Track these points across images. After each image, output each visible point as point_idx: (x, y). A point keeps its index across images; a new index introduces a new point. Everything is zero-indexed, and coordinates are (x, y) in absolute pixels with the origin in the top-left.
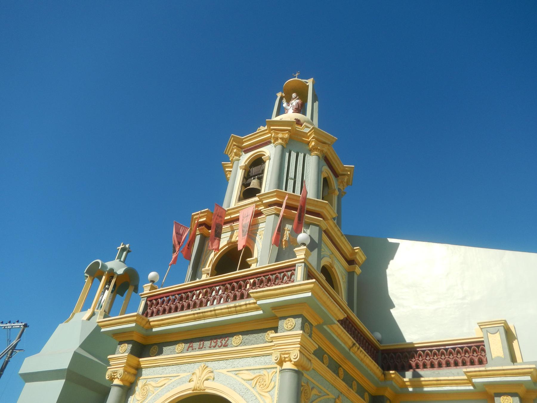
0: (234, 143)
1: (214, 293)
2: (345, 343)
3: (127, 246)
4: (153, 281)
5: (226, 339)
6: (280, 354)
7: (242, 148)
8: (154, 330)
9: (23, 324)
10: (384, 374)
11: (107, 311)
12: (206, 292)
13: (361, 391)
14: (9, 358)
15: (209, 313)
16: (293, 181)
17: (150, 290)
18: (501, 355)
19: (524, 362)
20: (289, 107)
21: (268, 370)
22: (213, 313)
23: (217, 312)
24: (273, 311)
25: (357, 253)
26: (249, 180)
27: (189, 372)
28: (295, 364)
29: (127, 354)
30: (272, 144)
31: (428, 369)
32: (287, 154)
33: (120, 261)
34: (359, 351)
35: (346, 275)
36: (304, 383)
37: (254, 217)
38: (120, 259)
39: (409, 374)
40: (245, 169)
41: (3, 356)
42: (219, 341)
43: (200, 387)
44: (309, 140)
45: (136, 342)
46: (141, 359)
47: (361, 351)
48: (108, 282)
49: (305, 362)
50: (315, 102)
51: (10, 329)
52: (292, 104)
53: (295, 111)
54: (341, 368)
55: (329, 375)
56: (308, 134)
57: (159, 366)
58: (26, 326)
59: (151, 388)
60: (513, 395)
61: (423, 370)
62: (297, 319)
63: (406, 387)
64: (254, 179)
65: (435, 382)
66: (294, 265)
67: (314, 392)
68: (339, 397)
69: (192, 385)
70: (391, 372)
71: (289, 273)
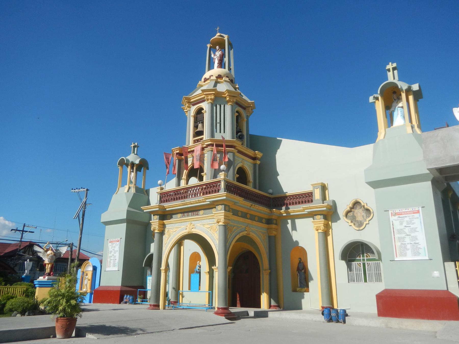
0: (186, 101)
1: (189, 192)
2: (248, 206)
3: (136, 144)
4: (160, 185)
5: (197, 212)
7: (191, 103)
8: (167, 209)
9: (86, 189)
10: (270, 210)
11: (135, 184)
12: (186, 191)
13: (260, 220)
14: (85, 209)
15: (188, 203)
16: (219, 124)
17: (161, 190)
19: (330, 199)
20: (215, 57)
21: (215, 224)
22: (190, 203)
23: (191, 202)
24: (213, 203)
25: (257, 154)
26: (197, 124)
27: (185, 225)
28: (223, 223)
29: (158, 220)
30: (206, 102)
32: (215, 107)
33: (135, 154)
34: (255, 207)
35: (251, 165)
36: (230, 226)
37: (202, 151)
38: (134, 153)
39: (284, 208)
40: (194, 117)
41: (81, 208)
42: (195, 212)
44: (226, 96)
45: (161, 215)
46: (164, 221)
47: (256, 206)
48: (132, 168)
49: (227, 221)
50: (231, 50)
51: (78, 192)
52: (217, 55)
53: (219, 61)
54: (248, 214)
55: (242, 220)
56: (225, 93)
57: (172, 223)
58: (87, 190)
60: (320, 215)
62: (222, 206)
63: (282, 214)
64: (200, 123)
65: (293, 211)
66: (220, 181)
67: (235, 228)
68: (247, 226)
69: (187, 231)
70: (274, 210)
71: (219, 184)
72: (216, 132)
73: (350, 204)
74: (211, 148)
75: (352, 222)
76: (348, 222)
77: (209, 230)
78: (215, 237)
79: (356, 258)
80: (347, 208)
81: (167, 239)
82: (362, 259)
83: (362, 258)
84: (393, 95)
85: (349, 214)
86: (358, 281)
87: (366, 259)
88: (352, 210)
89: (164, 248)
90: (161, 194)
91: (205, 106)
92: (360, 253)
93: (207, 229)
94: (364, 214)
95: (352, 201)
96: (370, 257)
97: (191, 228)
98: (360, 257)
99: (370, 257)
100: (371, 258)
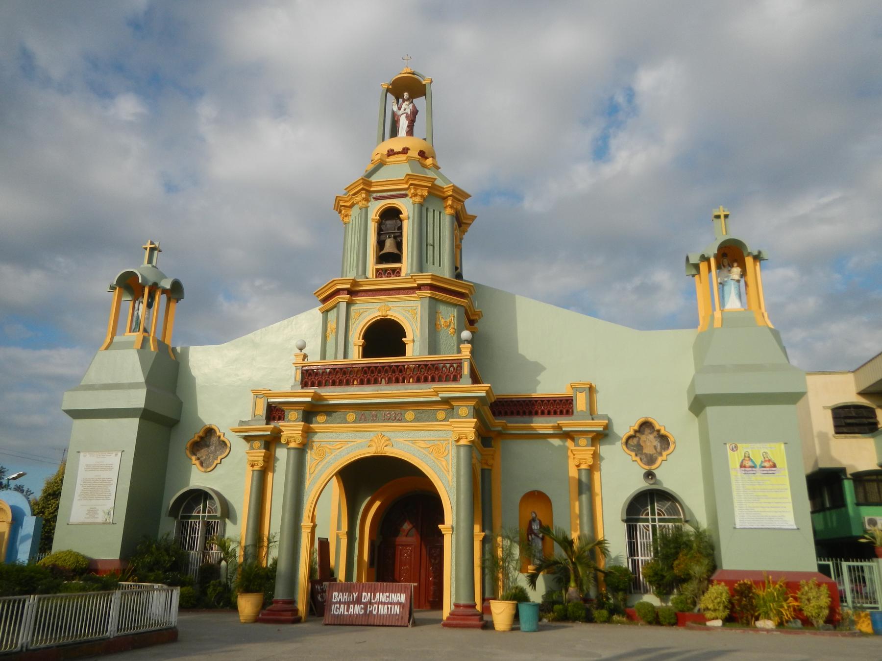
3: (157, 244)
6: (459, 434)
18: (584, 410)
30: (408, 198)
43: (381, 451)
46: (311, 425)
53: (410, 123)
57: (332, 432)
59: (327, 450)
64: (389, 237)
66: (461, 359)
72: (427, 262)
73: (635, 425)
74: (431, 293)
75: (636, 455)
77: (426, 453)
78: (441, 466)
79: (639, 516)
80: (628, 432)
81: (314, 465)
82: (652, 519)
83: (650, 517)
85: (630, 442)
86: (643, 555)
87: (659, 519)
88: (638, 435)
89: (307, 483)
90: (304, 368)
91: (406, 207)
93: (423, 451)
94: (657, 443)
95: (638, 422)
96: (664, 515)
97: (384, 445)
98: (647, 515)
99: (664, 515)
100: (666, 517)
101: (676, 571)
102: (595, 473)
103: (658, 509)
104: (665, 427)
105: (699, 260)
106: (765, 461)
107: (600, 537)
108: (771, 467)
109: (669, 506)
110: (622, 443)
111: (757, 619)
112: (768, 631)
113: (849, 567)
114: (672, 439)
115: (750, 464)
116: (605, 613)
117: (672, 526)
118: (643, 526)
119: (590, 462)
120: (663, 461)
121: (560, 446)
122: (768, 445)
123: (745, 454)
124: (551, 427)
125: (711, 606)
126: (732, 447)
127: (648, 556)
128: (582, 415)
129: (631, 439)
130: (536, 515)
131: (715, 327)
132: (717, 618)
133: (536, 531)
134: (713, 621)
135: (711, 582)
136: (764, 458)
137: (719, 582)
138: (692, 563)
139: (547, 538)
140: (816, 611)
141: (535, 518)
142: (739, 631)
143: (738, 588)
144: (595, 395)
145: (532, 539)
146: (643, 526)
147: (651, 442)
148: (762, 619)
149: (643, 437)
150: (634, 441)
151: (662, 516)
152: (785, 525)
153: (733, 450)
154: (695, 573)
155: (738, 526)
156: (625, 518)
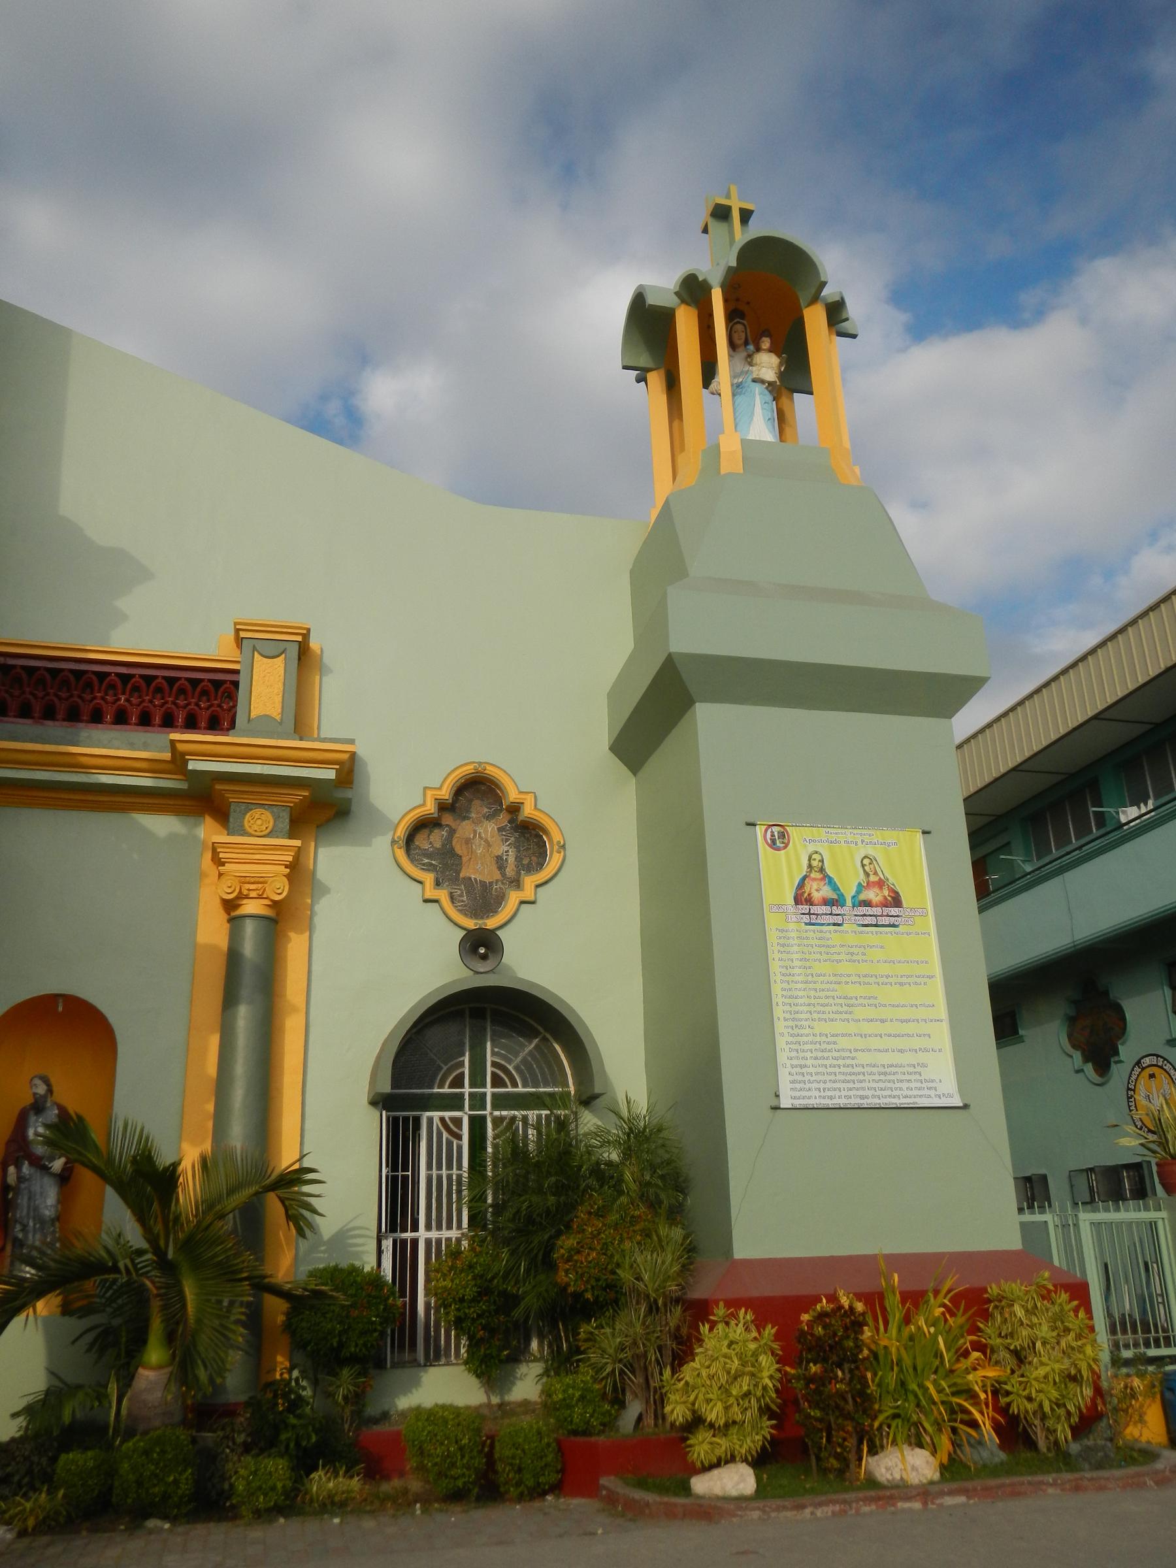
18: (275, 713)
31: (57, 723)
61: (42, 724)
75: (438, 884)
76: (420, 882)
79: (433, 1089)
80: (420, 806)
84: (745, 322)
85: (421, 841)
87: (494, 1095)
88: (447, 819)
92: (461, 1059)
96: (515, 1085)
98: (458, 1082)
99: (515, 1085)
100: (520, 1089)
101: (565, 1276)
102: (292, 935)
103: (494, 1064)
104: (535, 797)
105: (676, 293)
106: (869, 885)
107: (287, 1158)
108: (885, 904)
109: (530, 1053)
110: (393, 842)
111: (873, 1451)
112: (925, 1493)
113: (1096, 1225)
114: (556, 837)
115: (826, 892)
116: (277, 1468)
117: (539, 1117)
118: (442, 1120)
119: (279, 888)
120: (523, 906)
121: (172, 838)
122: (878, 835)
123: (810, 859)
124: (144, 765)
125: (714, 1414)
126: (772, 832)
127: (449, 1227)
128: (265, 725)
129: (426, 831)
130: (50, 1091)
131: (723, 472)
132: (731, 1459)
133: (40, 1150)
134: (716, 1472)
135: (700, 1311)
136: (867, 875)
137: (734, 1304)
138: (627, 1245)
139: (86, 1177)
140: (1054, 1394)
141: (44, 1097)
142: (828, 1510)
143: (819, 1330)
144: (318, 677)
145: (21, 1179)
146: (442, 1120)
147: (489, 845)
148: (894, 1443)
149: (465, 829)
150: (436, 838)
151: (507, 1087)
152: (929, 1096)
153: (773, 844)
154: (639, 1278)
155: (785, 1103)
156: (386, 1087)
